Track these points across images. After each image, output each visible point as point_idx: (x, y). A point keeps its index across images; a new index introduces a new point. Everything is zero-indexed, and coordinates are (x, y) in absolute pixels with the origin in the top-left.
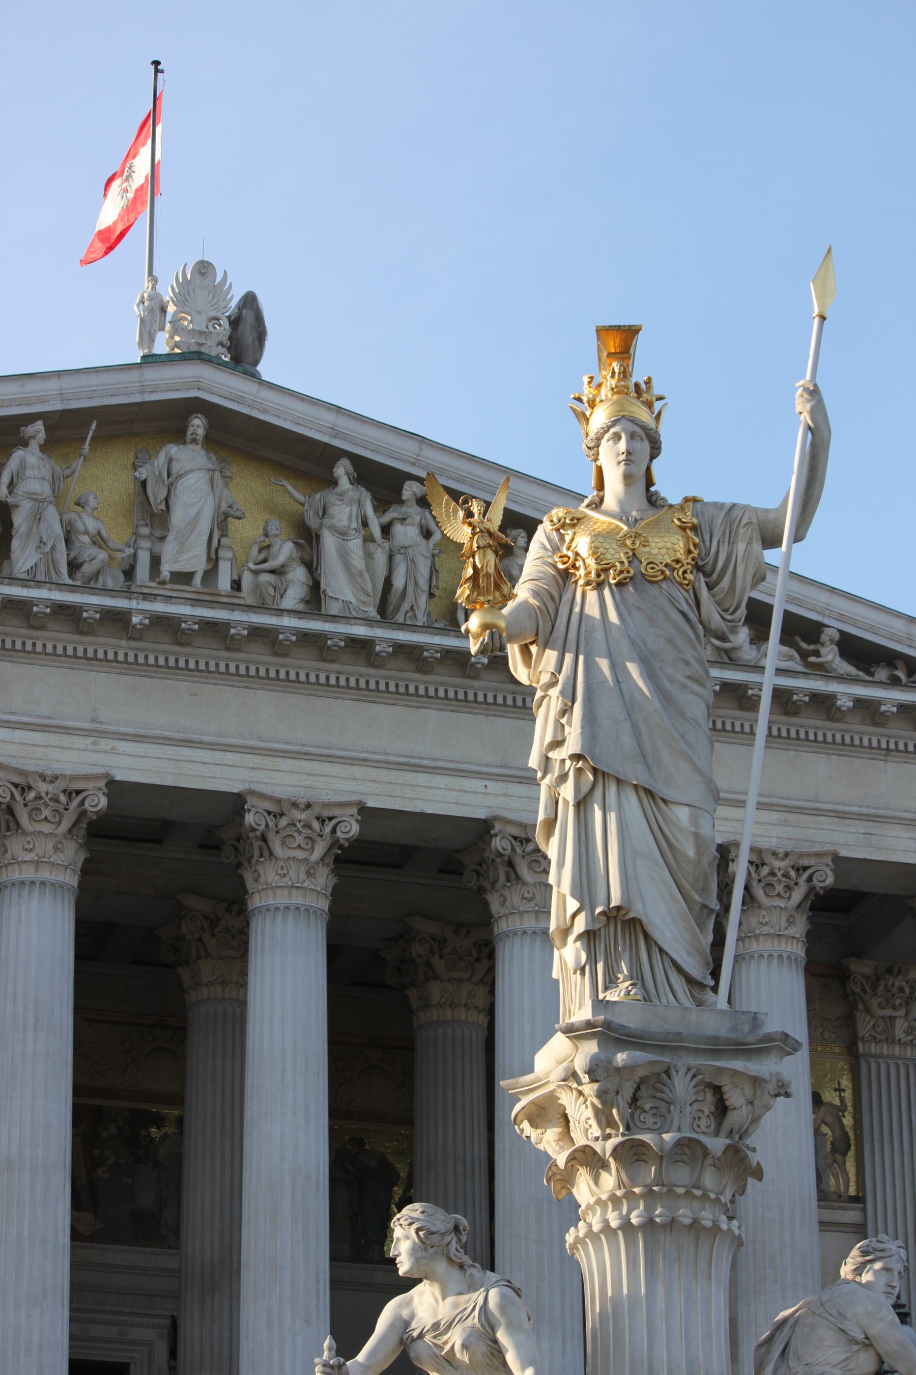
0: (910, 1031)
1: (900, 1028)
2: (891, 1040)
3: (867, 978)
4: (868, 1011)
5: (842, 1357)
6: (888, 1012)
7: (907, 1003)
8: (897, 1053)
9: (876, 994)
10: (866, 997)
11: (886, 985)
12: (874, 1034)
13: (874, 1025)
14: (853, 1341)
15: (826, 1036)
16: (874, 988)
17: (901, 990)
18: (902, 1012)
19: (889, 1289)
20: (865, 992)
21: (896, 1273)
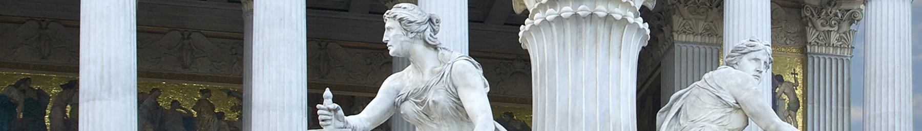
0: (840, 39)
1: (834, 38)
2: (827, 45)
3: (815, 8)
4: (814, 27)
5: (720, 115)
6: (827, 28)
7: (839, 23)
8: (831, 52)
9: (820, 17)
10: (814, 19)
11: (826, 13)
12: (818, 41)
13: (818, 35)
14: (727, 105)
15: (788, 43)
16: (819, 14)
17: (836, 15)
18: (836, 28)
19: (757, 73)
20: (813, 16)
21: (763, 62)
